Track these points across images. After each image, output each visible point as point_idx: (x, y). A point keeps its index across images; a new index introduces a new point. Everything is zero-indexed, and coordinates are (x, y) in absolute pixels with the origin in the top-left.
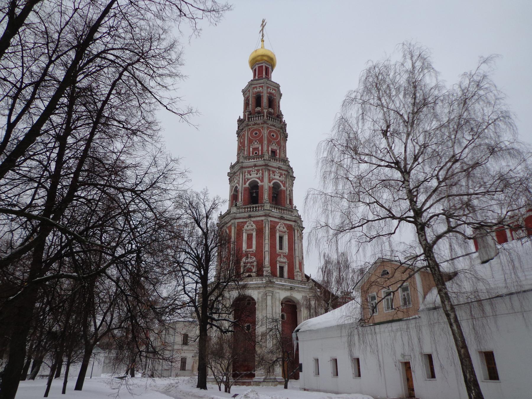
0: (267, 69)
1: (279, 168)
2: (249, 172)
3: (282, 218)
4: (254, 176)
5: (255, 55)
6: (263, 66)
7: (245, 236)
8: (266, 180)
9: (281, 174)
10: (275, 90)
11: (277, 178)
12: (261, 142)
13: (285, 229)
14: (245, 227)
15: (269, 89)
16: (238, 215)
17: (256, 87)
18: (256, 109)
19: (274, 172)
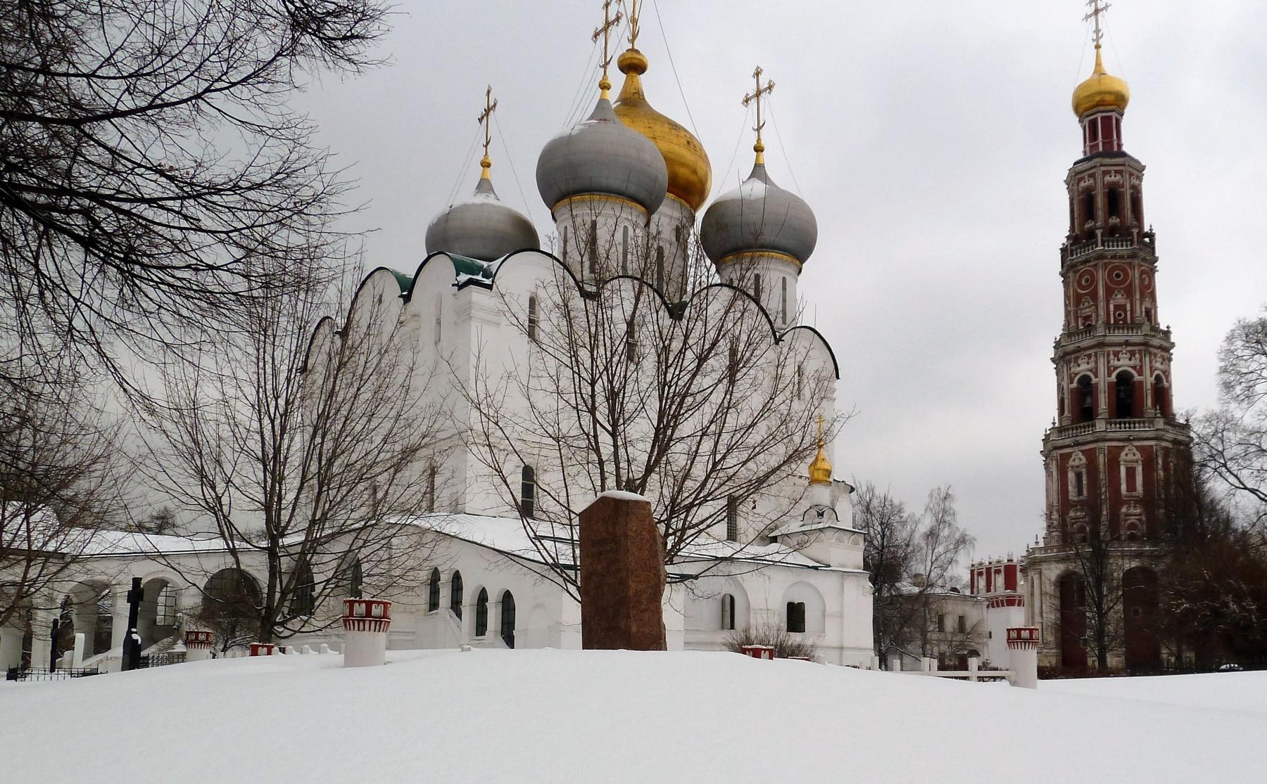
0: (1106, 121)
1: (1127, 344)
2: (1076, 359)
3: (1128, 440)
4: (1083, 367)
5: (1082, 87)
6: (1101, 114)
7: (1071, 476)
8: (1102, 370)
9: (1132, 354)
10: (1120, 172)
11: (1124, 363)
12: (1094, 296)
13: (1138, 456)
14: (1071, 463)
15: (1107, 178)
16: (1061, 443)
17: (1083, 178)
18: (1087, 226)
19: (1116, 354)
